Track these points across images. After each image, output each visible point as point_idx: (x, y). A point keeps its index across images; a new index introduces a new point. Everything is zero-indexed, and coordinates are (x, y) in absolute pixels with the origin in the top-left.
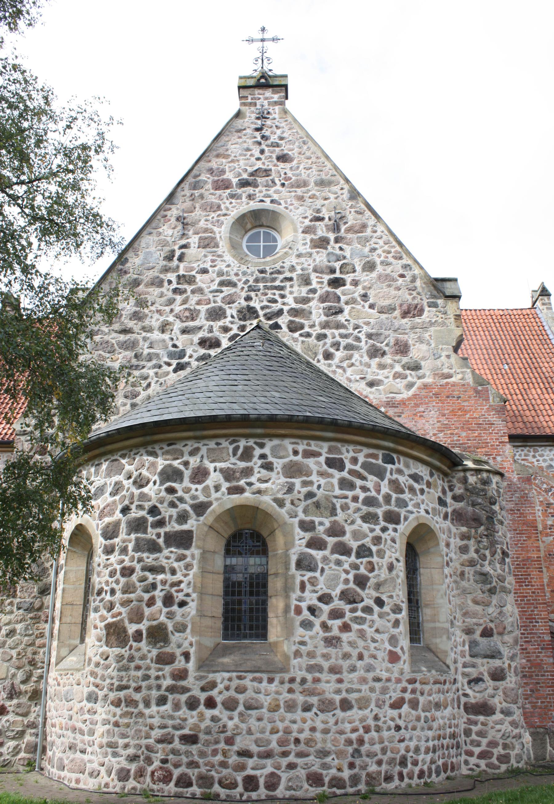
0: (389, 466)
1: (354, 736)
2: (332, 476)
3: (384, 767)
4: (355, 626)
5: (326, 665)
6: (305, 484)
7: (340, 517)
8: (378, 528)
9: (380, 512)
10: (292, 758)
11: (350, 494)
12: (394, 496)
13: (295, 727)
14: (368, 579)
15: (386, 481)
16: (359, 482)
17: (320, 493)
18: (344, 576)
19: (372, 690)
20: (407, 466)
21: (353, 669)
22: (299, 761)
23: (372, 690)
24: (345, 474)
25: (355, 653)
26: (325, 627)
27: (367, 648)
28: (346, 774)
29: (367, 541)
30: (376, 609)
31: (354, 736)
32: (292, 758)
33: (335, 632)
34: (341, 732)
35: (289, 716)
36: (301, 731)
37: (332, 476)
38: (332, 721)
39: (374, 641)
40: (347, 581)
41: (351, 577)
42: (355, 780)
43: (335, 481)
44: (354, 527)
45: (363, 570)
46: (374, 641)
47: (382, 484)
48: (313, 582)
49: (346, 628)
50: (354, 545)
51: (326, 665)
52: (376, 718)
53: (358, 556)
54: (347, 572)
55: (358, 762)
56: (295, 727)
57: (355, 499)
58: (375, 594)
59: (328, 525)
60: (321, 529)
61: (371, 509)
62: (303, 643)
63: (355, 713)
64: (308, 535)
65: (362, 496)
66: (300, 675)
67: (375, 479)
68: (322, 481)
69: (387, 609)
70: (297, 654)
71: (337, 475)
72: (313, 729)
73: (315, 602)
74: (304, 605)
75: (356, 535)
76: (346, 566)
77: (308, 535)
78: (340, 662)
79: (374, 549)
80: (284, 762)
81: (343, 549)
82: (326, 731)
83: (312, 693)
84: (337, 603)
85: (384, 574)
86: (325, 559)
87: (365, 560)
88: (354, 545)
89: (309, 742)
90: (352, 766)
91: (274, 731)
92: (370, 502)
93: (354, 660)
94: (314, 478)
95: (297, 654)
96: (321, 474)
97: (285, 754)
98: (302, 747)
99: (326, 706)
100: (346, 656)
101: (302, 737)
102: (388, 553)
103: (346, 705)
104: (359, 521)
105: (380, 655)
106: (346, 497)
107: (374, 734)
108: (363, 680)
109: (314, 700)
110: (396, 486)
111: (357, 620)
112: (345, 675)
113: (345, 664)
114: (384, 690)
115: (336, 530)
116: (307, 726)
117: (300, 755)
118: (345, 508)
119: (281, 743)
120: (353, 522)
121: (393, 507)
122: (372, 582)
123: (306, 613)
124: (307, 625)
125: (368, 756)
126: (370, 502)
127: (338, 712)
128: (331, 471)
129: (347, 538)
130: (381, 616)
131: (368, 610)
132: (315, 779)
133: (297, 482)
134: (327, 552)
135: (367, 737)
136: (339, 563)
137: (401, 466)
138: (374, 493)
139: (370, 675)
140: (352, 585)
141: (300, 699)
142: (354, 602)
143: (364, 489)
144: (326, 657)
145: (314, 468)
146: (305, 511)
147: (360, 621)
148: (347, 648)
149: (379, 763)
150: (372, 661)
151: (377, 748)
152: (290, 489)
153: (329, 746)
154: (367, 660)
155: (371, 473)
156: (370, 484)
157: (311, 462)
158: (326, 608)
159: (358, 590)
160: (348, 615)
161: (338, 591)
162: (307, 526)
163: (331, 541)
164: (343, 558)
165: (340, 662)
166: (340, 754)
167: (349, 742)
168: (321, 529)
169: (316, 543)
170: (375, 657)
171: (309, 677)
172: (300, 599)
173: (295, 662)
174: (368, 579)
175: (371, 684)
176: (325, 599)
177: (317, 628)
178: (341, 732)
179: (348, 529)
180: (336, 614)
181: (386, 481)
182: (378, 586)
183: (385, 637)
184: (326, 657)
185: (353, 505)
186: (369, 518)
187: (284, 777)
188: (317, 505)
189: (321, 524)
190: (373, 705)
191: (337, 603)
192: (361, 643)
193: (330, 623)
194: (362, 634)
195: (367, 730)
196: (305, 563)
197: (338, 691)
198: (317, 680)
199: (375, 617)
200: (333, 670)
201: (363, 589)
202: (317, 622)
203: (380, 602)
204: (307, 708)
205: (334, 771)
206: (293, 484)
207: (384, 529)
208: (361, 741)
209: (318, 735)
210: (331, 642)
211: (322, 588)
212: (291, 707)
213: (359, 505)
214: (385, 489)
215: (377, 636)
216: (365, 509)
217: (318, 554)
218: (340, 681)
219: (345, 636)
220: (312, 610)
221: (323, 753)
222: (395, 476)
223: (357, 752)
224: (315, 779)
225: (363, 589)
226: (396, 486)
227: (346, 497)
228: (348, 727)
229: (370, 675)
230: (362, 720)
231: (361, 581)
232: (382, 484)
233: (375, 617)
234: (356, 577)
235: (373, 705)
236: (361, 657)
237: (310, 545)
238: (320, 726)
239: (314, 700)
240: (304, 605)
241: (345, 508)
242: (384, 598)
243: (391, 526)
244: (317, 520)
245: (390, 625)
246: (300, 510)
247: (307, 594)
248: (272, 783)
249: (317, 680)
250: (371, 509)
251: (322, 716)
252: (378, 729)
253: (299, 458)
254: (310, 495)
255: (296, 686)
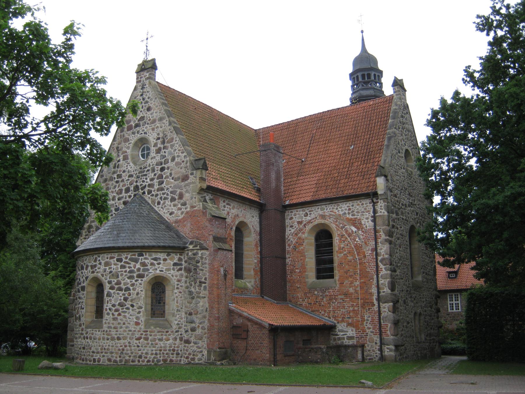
0: (140, 258)
1: (121, 348)
2: (118, 265)
3: (131, 358)
4: (123, 314)
5: (113, 326)
6: (110, 268)
7: (120, 278)
8: (134, 281)
9: (135, 275)
10: (103, 354)
11: (124, 270)
12: (142, 268)
13: (104, 345)
14: (128, 298)
15: (139, 263)
16: (127, 265)
17: (114, 271)
18: (120, 298)
19: (128, 334)
20: (150, 255)
21: (121, 328)
22: (106, 355)
23: (128, 334)
24: (122, 263)
25: (122, 323)
26: (113, 314)
27: (127, 321)
28: (118, 359)
29: (129, 286)
30: (131, 308)
31: (121, 348)
32: (103, 354)
33: (116, 316)
34: (117, 347)
35: (103, 342)
36: (106, 346)
37: (118, 265)
38: (114, 343)
39: (129, 318)
40: (120, 300)
41: (122, 298)
42: (121, 361)
43: (119, 266)
44: (125, 281)
45: (126, 295)
46: (129, 318)
47: (137, 265)
48: (110, 300)
49: (119, 315)
50: (124, 287)
51: (113, 326)
52: (129, 343)
53: (125, 291)
54: (121, 297)
55: (122, 356)
56: (104, 345)
57: (126, 271)
58: (131, 303)
59: (116, 281)
60: (113, 283)
61: (131, 274)
62: (107, 320)
63: (122, 341)
64: (110, 285)
65: (128, 270)
66: (106, 329)
67: (134, 263)
68: (115, 267)
69: (135, 308)
70: (105, 323)
71: (120, 264)
72: (109, 346)
73: (111, 307)
74: (108, 308)
75: (125, 284)
76: (121, 295)
77: (110, 285)
78: (117, 325)
79: (131, 288)
80: (102, 355)
81: (120, 289)
82: (113, 346)
83: (108, 335)
84: (117, 307)
85: (134, 296)
86: (114, 293)
87: (127, 292)
88: (124, 287)
89: (108, 349)
90: (120, 357)
91: (100, 346)
92: (131, 272)
93: (122, 325)
94: (113, 266)
95: (105, 323)
96: (115, 264)
97: (102, 353)
98: (106, 351)
99: (113, 339)
100: (119, 324)
101: (106, 348)
102: (137, 289)
103: (119, 339)
104: (127, 279)
105: (132, 323)
106: (122, 271)
107: (128, 348)
108: (125, 331)
109: (109, 337)
110: (144, 264)
111: (123, 312)
112: (119, 329)
113: (119, 326)
114: (133, 334)
115: (118, 283)
116: (108, 345)
117: (106, 353)
118: (122, 275)
119: (101, 349)
120: (124, 280)
121: (141, 272)
122: (130, 299)
123: (108, 310)
124: (108, 314)
125: (125, 354)
126: (131, 272)
127: (116, 340)
128: (118, 263)
129: (122, 286)
130: (133, 310)
131: (128, 309)
132: (109, 360)
133: (107, 268)
134: (115, 291)
135: (125, 349)
136: (118, 294)
137: (147, 256)
138: (133, 268)
139: (128, 329)
140: (122, 301)
141: (106, 336)
142: (123, 306)
143: (129, 267)
144: (113, 324)
145: (112, 262)
146: (109, 278)
147: (125, 312)
148: (119, 321)
149: (130, 356)
150: (128, 325)
151: (129, 352)
152: (105, 270)
153: (113, 351)
154: (126, 325)
155: (132, 261)
156: (132, 266)
157: (112, 261)
158: (114, 308)
159: (125, 302)
160: (121, 310)
161: (118, 303)
162: (110, 282)
163: (116, 286)
164: (120, 292)
165: (117, 325)
166: (117, 353)
167: (119, 350)
168: (113, 283)
169: (112, 288)
170: (129, 324)
171: (108, 330)
172: (107, 306)
173: (105, 325)
174: (128, 298)
175: (128, 332)
176: (114, 306)
177: (111, 315)
178: (117, 347)
179: (122, 282)
180: (116, 310)
181: (139, 263)
182: (132, 301)
183: (134, 317)
184: (113, 324)
185: (125, 274)
186: (131, 277)
187: (102, 359)
188: (113, 275)
189: (114, 281)
190: (128, 339)
191: (117, 307)
192: (124, 319)
193: (115, 313)
194: (125, 316)
195: (126, 346)
196: (109, 295)
197: (116, 334)
198: (110, 331)
199: (131, 310)
200: (115, 328)
201: (126, 301)
202: (111, 313)
203: (132, 306)
204: (108, 339)
205: (115, 358)
206: (106, 269)
207: (136, 281)
208: (123, 350)
209: (110, 348)
210: (114, 319)
211: (113, 302)
212: (104, 339)
213: (127, 273)
214: (138, 266)
215: (131, 317)
216: (129, 274)
217: (112, 291)
218: (117, 331)
219: (119, 317)
220: (110, 309)
221: (112, 353)
222: (143, 261)
223: (122, 353)
224: (109, 360)
225: (126, 301)
226: (144, 264)
227: (122, 271)
228: (119, 345)
229: (128, 329)
230: (124, 343)
231: (126, 299)
232: (137, 265)
233: (131, 310)
234: (124, 298)
235: (128, 339)
236: (124, 324)
237: (110, 289)
238: (111, 345)
239: (109, 337)
240: (108, 308)
241: (122, 275)
242: (135, 304)
243: (140, 279)
244: (113, 280)
245: (136, 313)
246: (108, 277)
247: (109, 304)
248: (99, 361)
249: (110, 331)
250: (131, 274)
251: (112, 342)
252: (130, 346)
253: (108, 260)
254: (111, 272)
255: (105, 333)
